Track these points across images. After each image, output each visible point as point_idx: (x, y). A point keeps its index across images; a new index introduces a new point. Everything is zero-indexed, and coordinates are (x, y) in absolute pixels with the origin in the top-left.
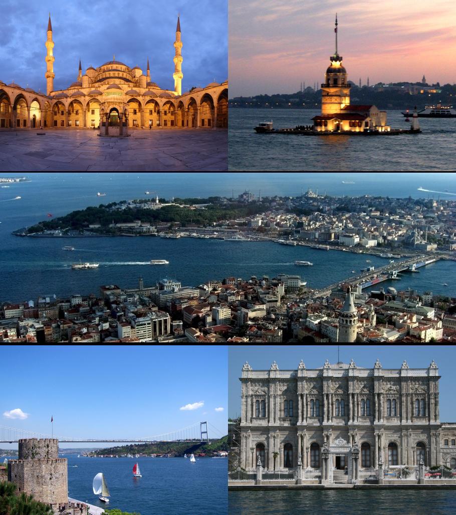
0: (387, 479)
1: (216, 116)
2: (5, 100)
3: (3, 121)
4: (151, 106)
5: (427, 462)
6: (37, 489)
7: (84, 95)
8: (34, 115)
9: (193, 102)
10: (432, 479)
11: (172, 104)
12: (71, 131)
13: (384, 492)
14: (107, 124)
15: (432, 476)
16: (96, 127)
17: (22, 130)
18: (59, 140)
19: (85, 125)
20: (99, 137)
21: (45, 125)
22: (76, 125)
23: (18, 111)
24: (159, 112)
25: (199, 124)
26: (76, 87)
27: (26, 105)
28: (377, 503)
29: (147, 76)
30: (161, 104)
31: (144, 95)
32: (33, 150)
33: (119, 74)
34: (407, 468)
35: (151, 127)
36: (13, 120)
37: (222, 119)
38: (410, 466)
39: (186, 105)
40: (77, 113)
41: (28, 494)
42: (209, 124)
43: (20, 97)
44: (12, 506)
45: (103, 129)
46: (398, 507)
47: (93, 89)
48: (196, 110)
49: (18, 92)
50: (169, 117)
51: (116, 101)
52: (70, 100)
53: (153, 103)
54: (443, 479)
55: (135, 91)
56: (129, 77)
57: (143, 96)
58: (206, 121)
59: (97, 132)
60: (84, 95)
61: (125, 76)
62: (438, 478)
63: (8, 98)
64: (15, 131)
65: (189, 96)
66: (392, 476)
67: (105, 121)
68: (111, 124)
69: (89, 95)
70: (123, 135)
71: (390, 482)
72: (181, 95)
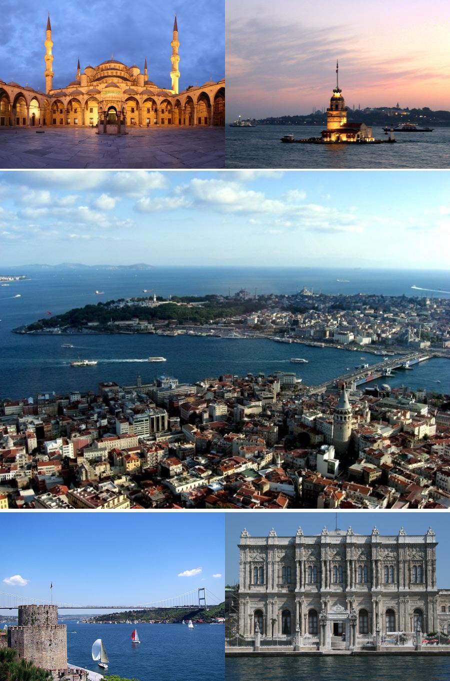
0: (385, 645)
1: (212, 114)
2: (4, 99)
3: (3, 119)
4: (149, 104)
5: (424, 628)
6: (37, 655)
7: (83, 94)
8: (34, 114)
9: (190, 100)
10: (429, 645)
11: (169, 103)
12: (70, 129)
13: (381, 659)
14: (105, 122)
15: (429, 643)
16: (95, 125)
17: (22, 128)
18: (58, 138)
19: (84, 123)
20: (97, 135)
21: (44, 123)
22: (75, 123)
23: (18, 109)
24: (156, 111)
25: (196, 122)
26: (75, 86)
27: (25, 104)
28: (374, 669)
29: (145, 75)
30: (158, 102)
31: (142, 94)
32: (33, 148)
33: (117, 73)
34: (404, 635)
35: (148, 126)
36: (13, 118)
37: (219, 117)
38: (407, 633)
39: (183, 104)
40: (76, 111)
41: (28, 660)
42: (206, 123)
43: (19, 96)
44: (12, 672)
45: (102, 127)
46: (395, 673)
47: (91, 88)
48: (192, 108)
49: (17, 91)
50: (167, 116)
51: (114, 99)
52: (68, 99)
53: (150, 101)
54: (440, 645)
55: (133, 90)
56: (127, 76)
57: (140, 94)
58: (203, 119)
59: (95, 130)
60: (83, 94)
61: (122, 75)
62: (435, 645)
63: (7, 97)
64: (14, 129)
65: (186, 95)
66: (390, 642)
67: (103, 119)
68: (109, 122)
69: (87, 94)
70: (121, 134)
71: (387, 648)
72: (177, 93)
